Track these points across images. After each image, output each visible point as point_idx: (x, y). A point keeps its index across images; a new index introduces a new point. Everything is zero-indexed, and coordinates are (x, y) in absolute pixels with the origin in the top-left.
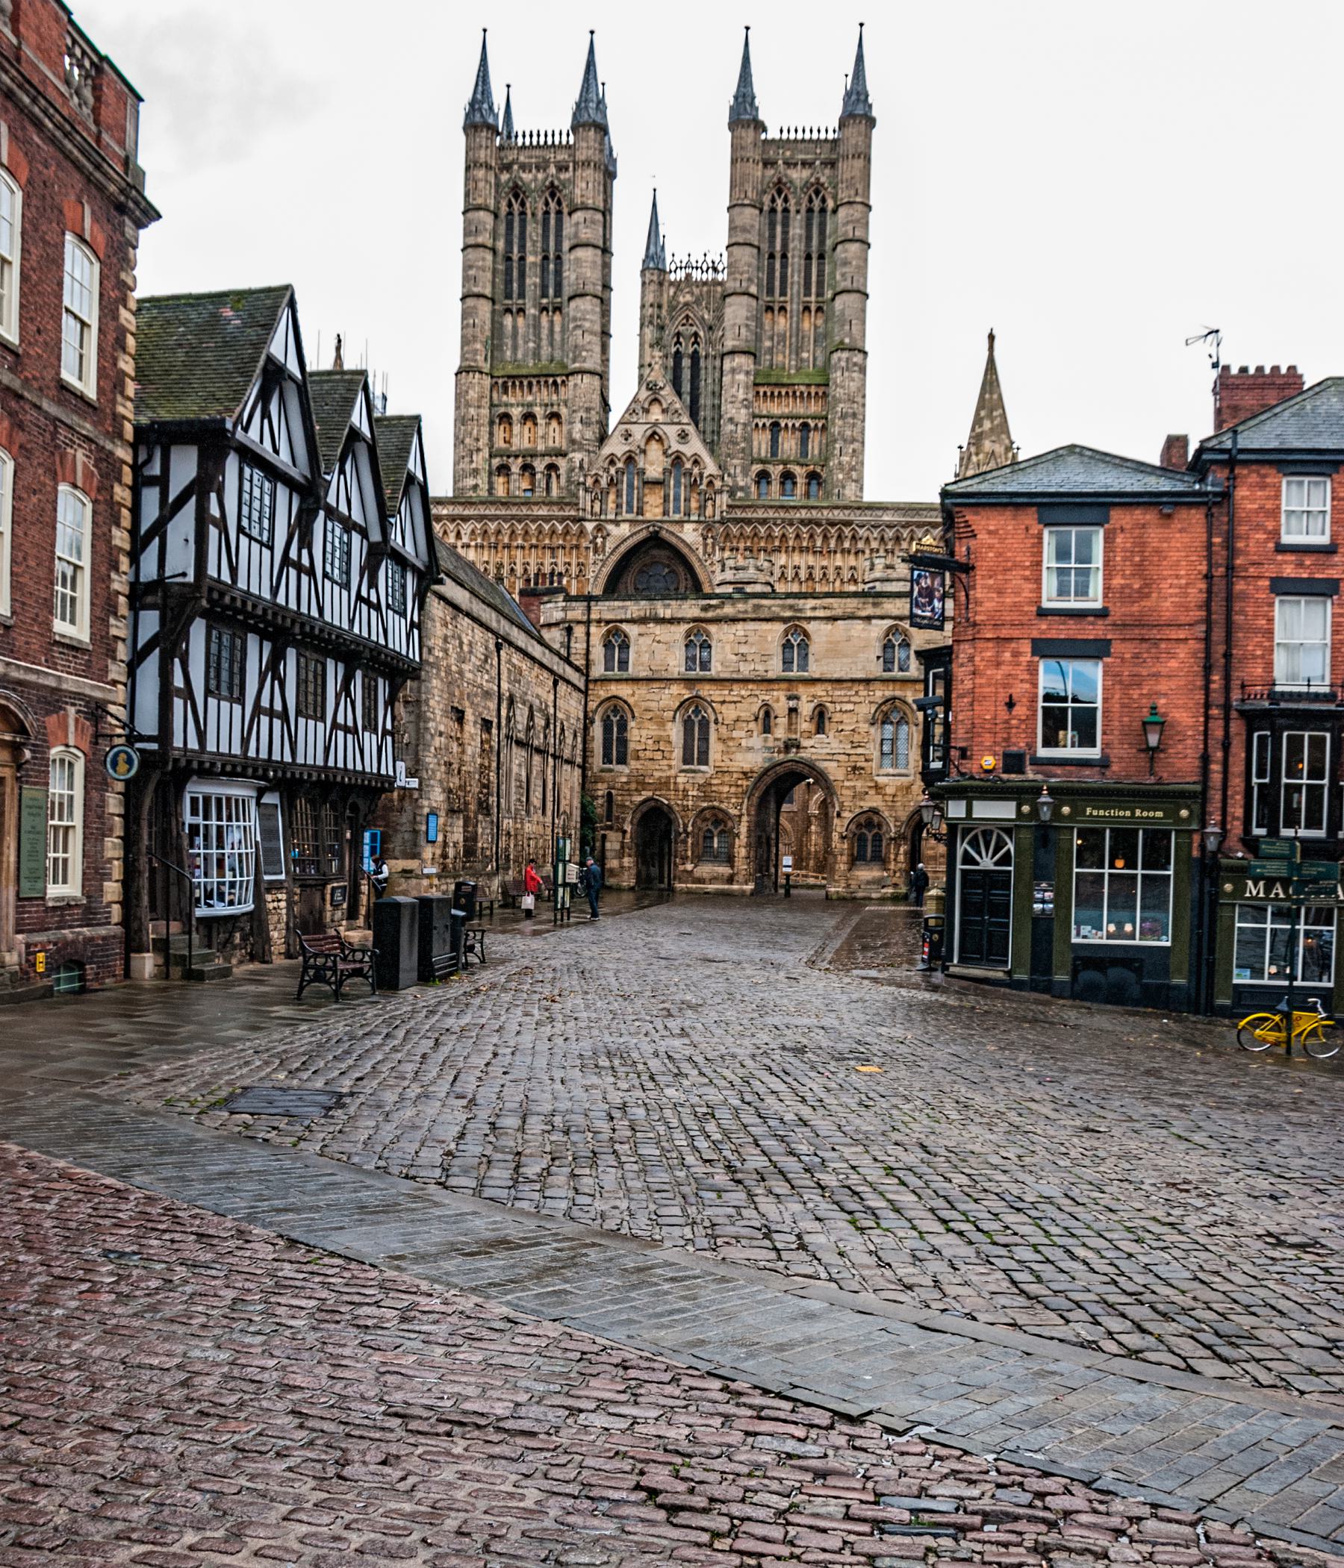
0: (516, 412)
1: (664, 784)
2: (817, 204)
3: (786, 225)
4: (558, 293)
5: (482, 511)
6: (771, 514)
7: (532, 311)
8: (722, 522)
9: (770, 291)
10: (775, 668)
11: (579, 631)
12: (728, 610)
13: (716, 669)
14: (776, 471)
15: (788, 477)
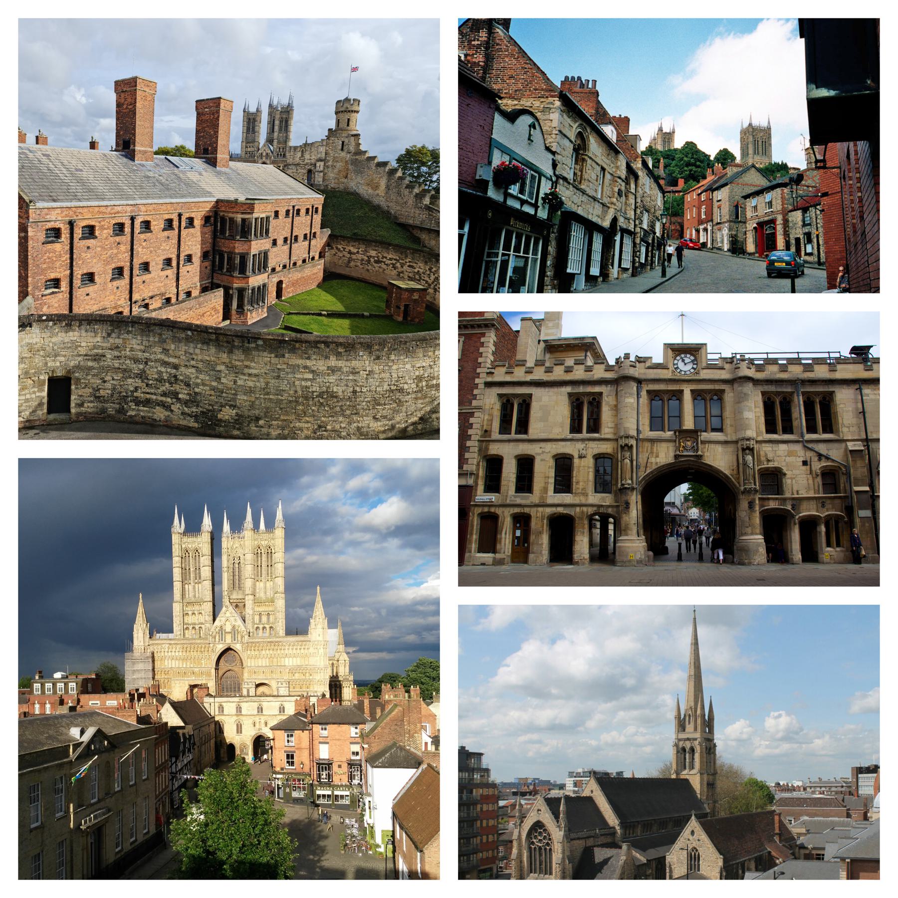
0: (190, 613)
1: (232, 738)
2: (269, 551)
3: (261, 557)
4: (200, 578)
5: (182, 642)
6: (260, 640)
7: (192, 584)
8: (247, 643)
9: (258, 576)
10: (255, 712)
11: (212, 704)
12: (245, 700)
13: (243, 712)
14: (261, 626)
15: (264, 628)
